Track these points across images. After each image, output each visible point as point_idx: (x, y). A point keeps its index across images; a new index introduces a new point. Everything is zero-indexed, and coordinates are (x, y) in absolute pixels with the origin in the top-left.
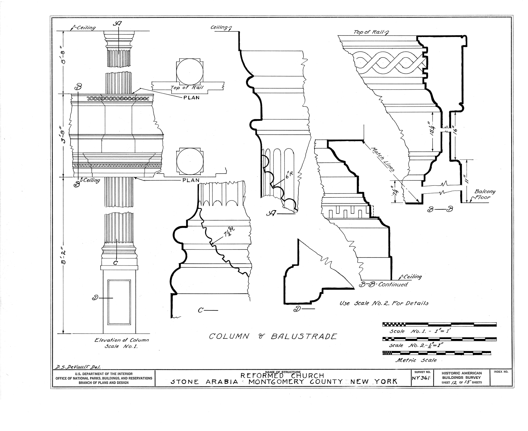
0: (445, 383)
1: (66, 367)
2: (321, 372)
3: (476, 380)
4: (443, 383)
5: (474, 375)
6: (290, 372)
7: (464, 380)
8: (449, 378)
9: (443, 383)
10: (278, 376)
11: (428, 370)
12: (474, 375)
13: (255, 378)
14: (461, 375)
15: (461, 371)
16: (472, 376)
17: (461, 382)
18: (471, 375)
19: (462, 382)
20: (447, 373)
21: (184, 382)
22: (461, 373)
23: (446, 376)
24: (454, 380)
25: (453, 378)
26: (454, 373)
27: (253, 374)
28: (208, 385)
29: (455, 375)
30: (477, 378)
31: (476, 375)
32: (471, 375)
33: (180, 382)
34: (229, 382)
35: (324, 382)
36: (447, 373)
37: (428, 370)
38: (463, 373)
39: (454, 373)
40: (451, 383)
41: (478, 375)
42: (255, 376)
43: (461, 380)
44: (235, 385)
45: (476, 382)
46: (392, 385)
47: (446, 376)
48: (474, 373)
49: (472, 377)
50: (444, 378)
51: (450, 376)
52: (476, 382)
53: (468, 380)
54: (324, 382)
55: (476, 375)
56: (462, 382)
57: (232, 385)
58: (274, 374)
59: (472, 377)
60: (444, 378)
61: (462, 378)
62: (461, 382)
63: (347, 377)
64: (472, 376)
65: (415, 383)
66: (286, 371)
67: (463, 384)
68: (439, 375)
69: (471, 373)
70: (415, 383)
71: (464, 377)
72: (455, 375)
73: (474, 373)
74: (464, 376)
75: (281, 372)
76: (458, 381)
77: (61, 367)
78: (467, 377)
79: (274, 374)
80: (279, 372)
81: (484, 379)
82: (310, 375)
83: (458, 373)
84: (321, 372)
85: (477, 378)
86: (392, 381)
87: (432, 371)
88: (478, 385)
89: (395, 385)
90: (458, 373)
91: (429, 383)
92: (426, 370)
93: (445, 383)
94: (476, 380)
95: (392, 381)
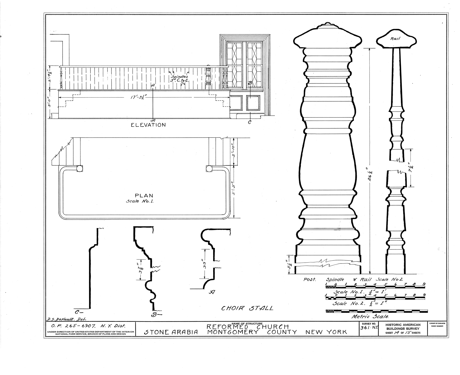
0: (389, 333)
1: (55, 319)
2: (286, 324)
3: (415, 331)
4: (386, 333)
5: (414, 327)
6: (253, 324)
7: (405, 331)
8: (392, 329)
9: (386, 333)
10: (243, 327)
11: (373, 322)
12: (414, 327)
13: (220, 329)
14: (402, 327)
15: (402, 323)
16: (412, 327)
17: (402, 333)
18: (411, 327)
19: (403, 333)
20: (390, 325)
21: (157, 332)
22: (402, 325)
23: (389, 327)
24: (397, 331)
25: (395, 330)
26: (397, 325)
27: (218, 326)
28: (174, 335)
29: (397, 327)
30: (416, 329)
31: (416, 327)
32: (411, 327)
33: (153, 332)
34: (191, 332)
35: (279, 332)
36: (390, 325)
37: (373, 322)
39: (397, 325)
40: (393, 333)
41: (417, 327)
42: (220, 327)
43: (402, 331)
44: (196, 335)
45: (415, 333)
46: (342, 335)
47: (389, 327)
48: (414, 325)
49: (412, 328)
50: (388, 329)
51: (394, 327)
52: (415, 333)
53: (408, 331)
54: (279, 332)
55: (416, 327)
56: (403, 333)
57: (193, 335)
58: (239, 326)
59: (412, 328)
60: (388, 329)
61: (404, 329)
62: (402, 333)
63: (301, 329)
64: (412, 327)
65: (363, 332)
66: (251, 322)
67: (404, 334)
68: (383, 327)
69: (411, 325)
70: (363, 332)
71: (405, 329)
72: (397, 327)
73: (414, 325)
74: (406, 327)
75: (245, 324)
76: (400, 331)
77: (51, 319)
78: (407, 329)
79: (239, 326)
80: (243, 324)
81: (422, 330)
82: (275, 326)
83: (400, 325)
84: (286, 324)
85: (416, 329)
86: (342, 332)
87: (377, 323)
88: (417, 335)
89: (345, 334)
90: (400, 325)
91: (374, 332)
92: (372, 322)
93: (389, 333)
94: (415, 331)
95: (342, 332)
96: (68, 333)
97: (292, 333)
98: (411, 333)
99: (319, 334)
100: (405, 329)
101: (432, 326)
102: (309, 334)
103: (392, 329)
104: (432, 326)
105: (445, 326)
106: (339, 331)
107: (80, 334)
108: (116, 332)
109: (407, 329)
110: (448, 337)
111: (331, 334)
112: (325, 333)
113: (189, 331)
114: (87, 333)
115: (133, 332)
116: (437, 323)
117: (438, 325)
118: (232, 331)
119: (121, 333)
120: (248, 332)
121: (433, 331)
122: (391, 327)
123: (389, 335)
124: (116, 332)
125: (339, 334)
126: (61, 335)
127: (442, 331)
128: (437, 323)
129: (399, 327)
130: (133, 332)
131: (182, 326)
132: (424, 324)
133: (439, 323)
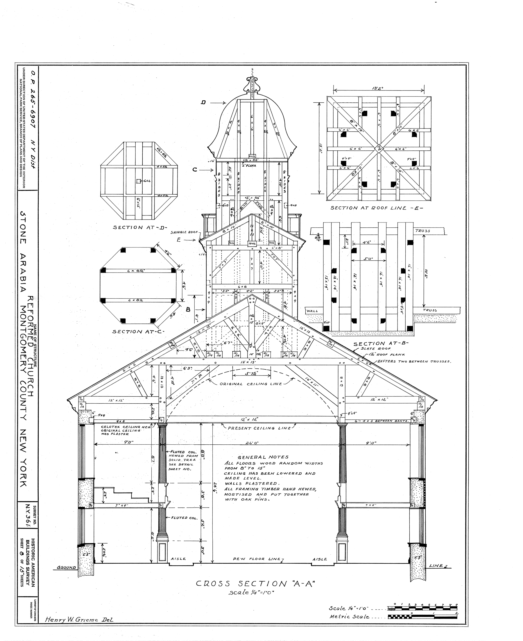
0: (22, 543)
5: (30, 578)
7: (25, 566)
8: (28, 547)
11: (37, 522)
12: (30, 578)
14: (31, 562)
15: (35, 562)
18: (31, 574)
19: (22, 563)
20: (33, 545)
22: (33, 562)
24: (25, 554)
26: (33, 554)
29: (31, 554)
30: (28, 580)
32: (31, 574)
33: (23, 222)
36: (33, 545)
38: (33, 564)
39: (33, 554)
41: (31, 582)
43: (25, 562)
45: (22, 579)
46: (19, 480)
48: (33, 578)
49: (28, 575)
50: (28, 541)
51: (30, 550)
52: (22, 579)
53: (25, 570)
59: (28, 575)
60: (28, 541)
63: (28, 425)
65: (22, 506)
67: (20, 564)
69: (33, 574)
70: (22, 506)
71: (28, 566)
72: (31, 554)
73: (33, 578)
74: (30, 566)
76: (24, 557)
78: (28, 569)
81: (27, 590)
83: (33, 558)
85: (28, 580)
86: (23, 479)
88: (19, 582)
89: (20, 484)
90: (33, 558)
91: (22, 523)
92: (37, 519)
93: (22, 543)
95: (23, 479)
96: (22, 96)
97: (21, 414)
98: (22, 574)
99: (20, 447)
100: (28, 566)
101: (31, 603)
103: (28, 547)
104: (31, 603)
105: (32, 621)
106: (25, 476)
107: (21, 127)
108: (23, 163)
110: (16, 625)
111: (20, 464)
112: (22, 456)
113: (24, 278)
114: (22, 123)
115: (24, 187)
116: (35, 609)
117: (33, 611)
118: (25, 338)
119: (23, 171)
120: (23, 359)
121: (25, 605)
122: (31, 546)
123: (19, 542)
124: (23, 163)
125: (20, 476)
126: (20, 87)
127: (25, 617)
128: (35, 609)
129: (30, 557)
130: (24, 187)
132: (33, 592)
133: (36, 606)
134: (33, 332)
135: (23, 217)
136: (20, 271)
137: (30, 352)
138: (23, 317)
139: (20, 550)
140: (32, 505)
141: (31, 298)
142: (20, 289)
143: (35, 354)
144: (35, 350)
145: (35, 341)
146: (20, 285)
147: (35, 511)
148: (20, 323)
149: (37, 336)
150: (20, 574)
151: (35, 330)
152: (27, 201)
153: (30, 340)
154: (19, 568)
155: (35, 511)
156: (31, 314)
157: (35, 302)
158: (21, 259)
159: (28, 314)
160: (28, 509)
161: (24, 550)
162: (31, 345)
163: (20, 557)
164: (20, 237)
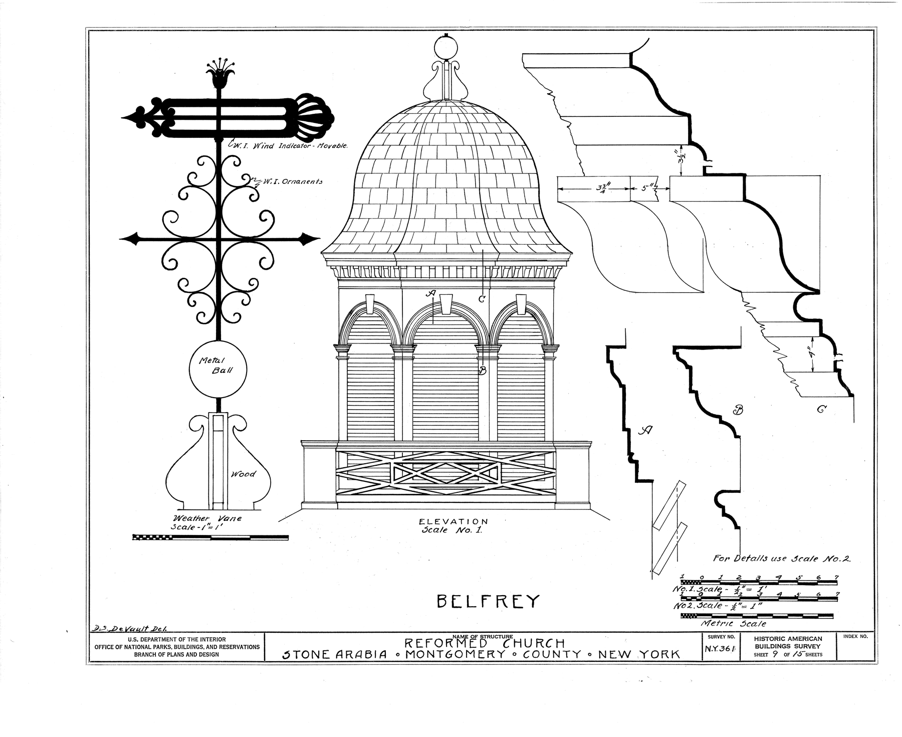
0: (760, 655)
3: (811, 651)
4: (756, 655)
5: (810, 643)
7: (792, 650)
8: (766, 647)
9: (756, 655)
11: (730, 634)
12: (810, 643)
14: (786, 642)
15: (787, 635)
17: (787, 655)
18: (805, 642)
20: (763, 639)
21: (306, 655)
22: (786, 639)
23: (761, 643)
29: (775, 642)
32: (805, 642)
33: (299, 654)
36: (763, 639)
37: (730, 634)
39: (776, 638)
43: (787, 650)
45: (812, 655)
47: (761, 643)
49: (805, 646)
50: (757, 646)
51: (769, 643)
52: (812, 655)
53: (799, 650)
59: (805, 646)
60: (757, 646)
61: (789, 646)
62: (787, 655)
65: (708, 656)
67: (790, 658)
68: (749, 641)
69: (804, 638)
70: (708, 656)
71: (792, 646)
72: (775, 642)
74: (792, 643)
76: (781, 651)
78: (796, 646)
81: (827, 648)
83: (781, 639)
86: (669, 654)
87: (737, 635)
88: (816, 659)
89: (675, 658)
90: (781, 639)
92: (727, 634)
93: (760, 655)
94: (811, 651)
95: (669, 654)
99: (625, 658)
102: (605, 658)
106: (664, 653)
109: (796, 646)
122: (765, 642)
123: (760, 660)
131: (617, 643)
132: (829, 638)
134: (462, 640)
135: (293, 655)
136: (358, 659)
137: (495, 644)
138: (420, 654)
139: (770, 657)
140: (708, 642)
141: (408, 643)
142: (383, 658)
143: (495, 637)
144: (489, 637)
145: (476, 636)
146: (378, 659)
147: (715, 637)
148: (431, 658)
149: (470, 635)
150: (803, 657)
151: (462, 637)
152: (276, 647)
153: (476, 643)
154: (797, 658)
155: (715, 637)
156: (432, 642)
157: (414, 637)
158: (345, 657)
159: (431, 647)
160: (712, 648)
161: (770, 651)
162: (483, 642)
163: (780, 656)
164: (320, 658)
